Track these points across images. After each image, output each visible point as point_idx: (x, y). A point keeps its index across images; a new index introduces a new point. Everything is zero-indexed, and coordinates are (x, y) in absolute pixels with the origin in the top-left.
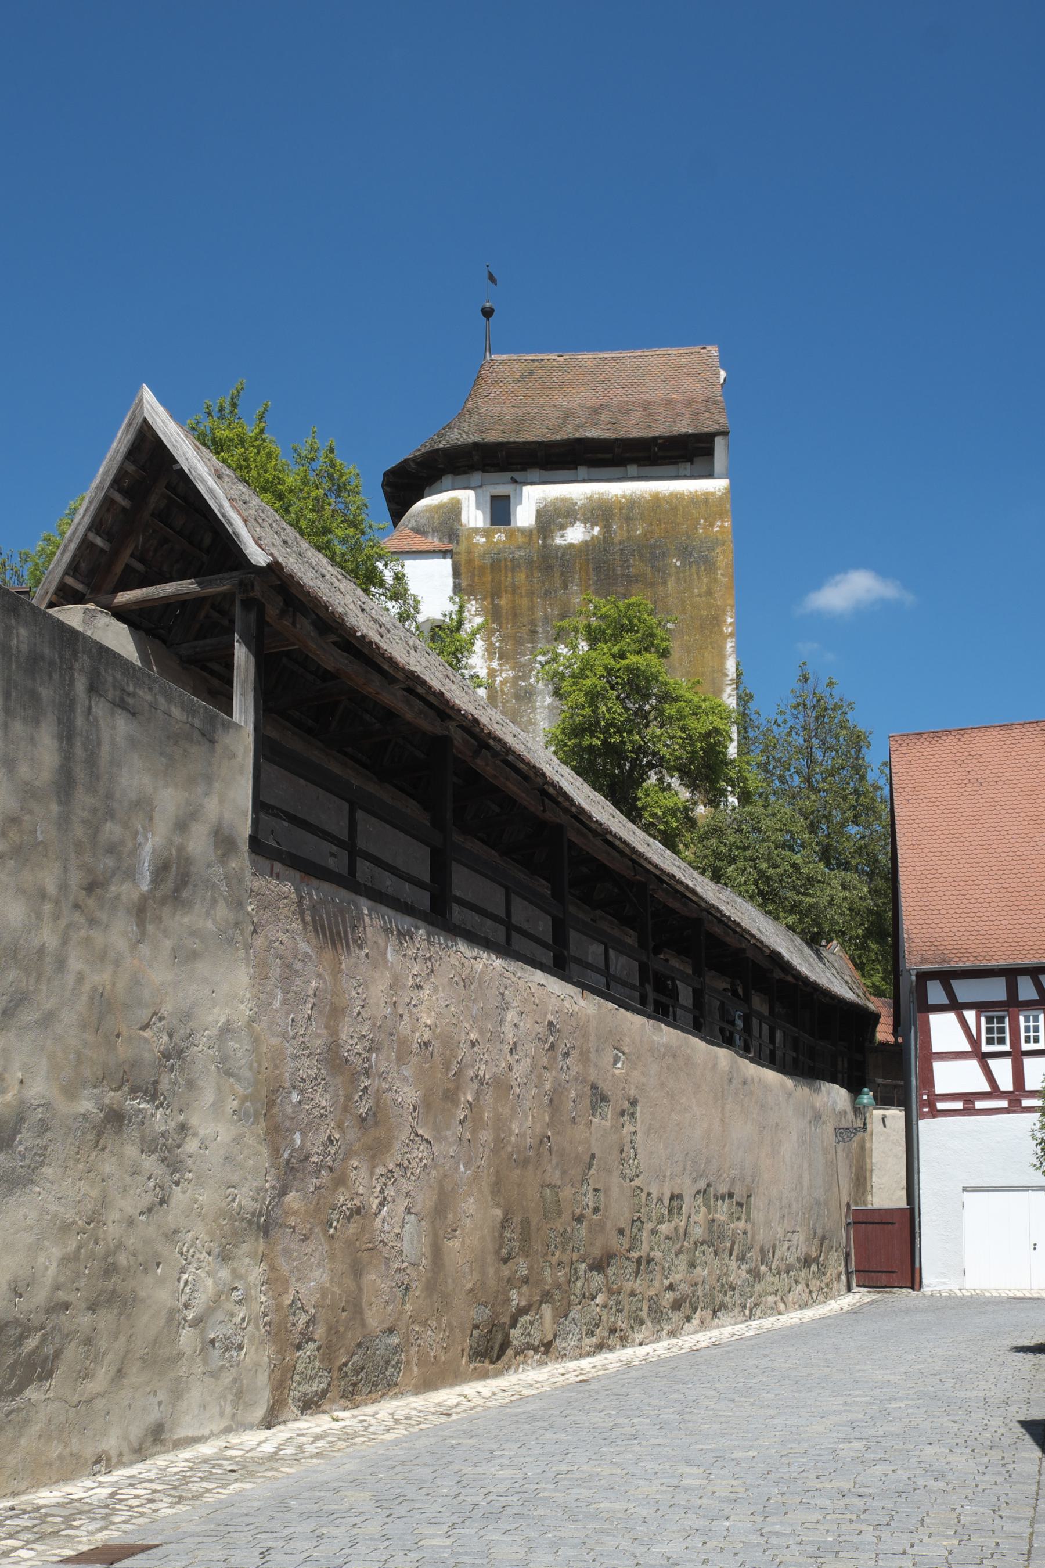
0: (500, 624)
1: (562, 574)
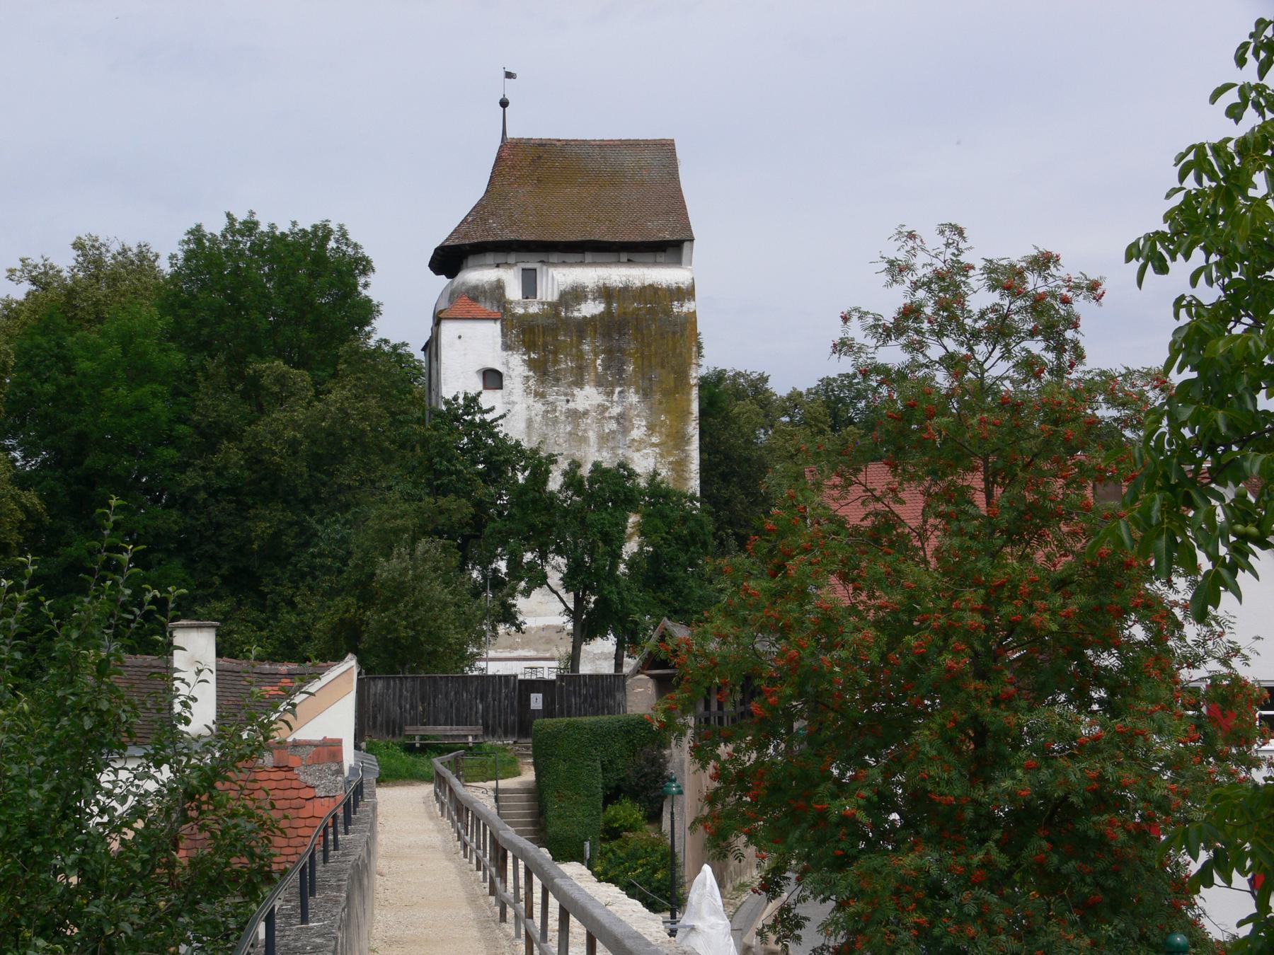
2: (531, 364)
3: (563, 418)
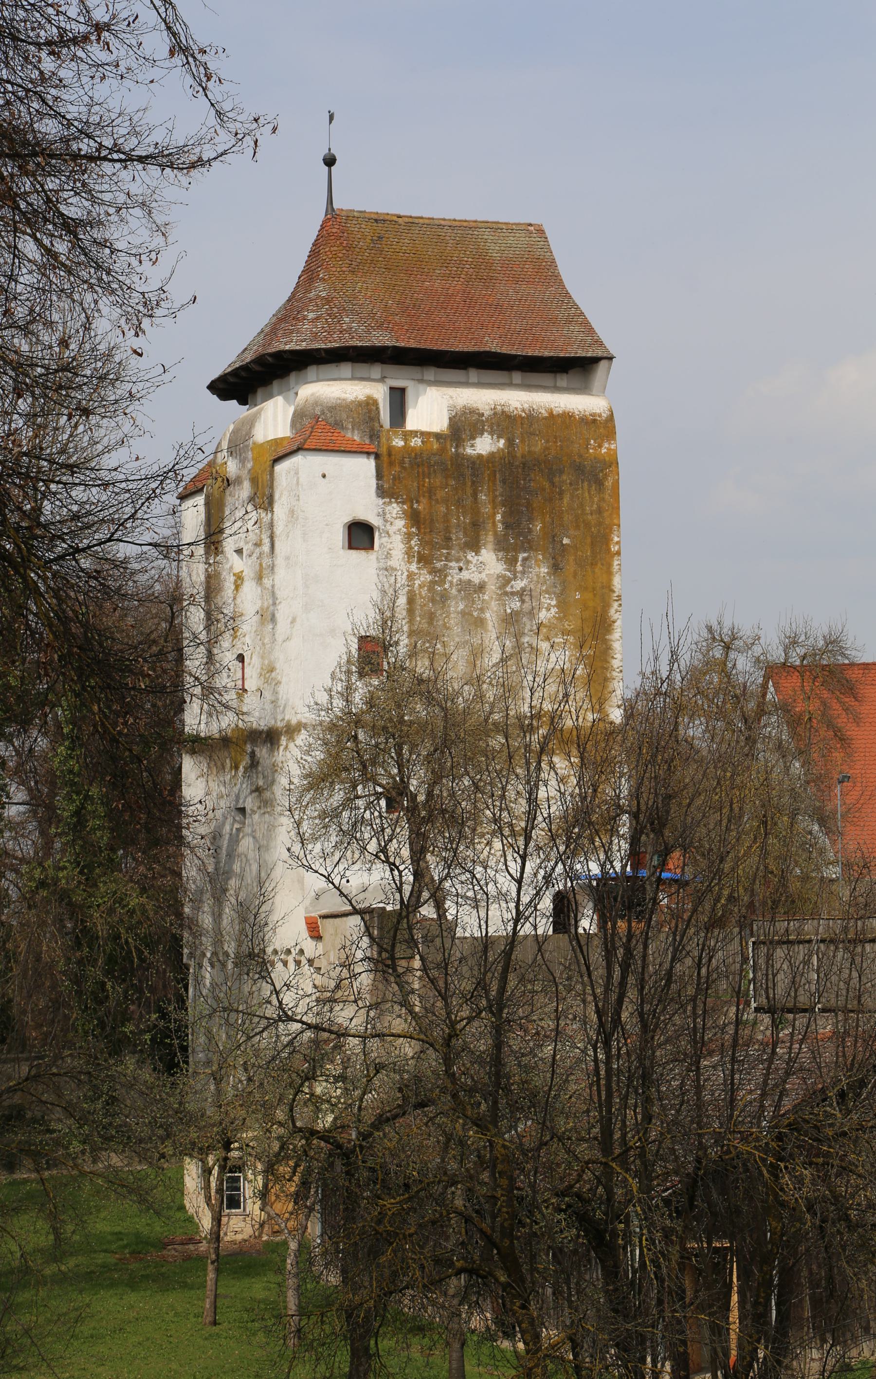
0: (418, 528)
1: (473, 483)
2: (414, 518)
3: (454, 591)
